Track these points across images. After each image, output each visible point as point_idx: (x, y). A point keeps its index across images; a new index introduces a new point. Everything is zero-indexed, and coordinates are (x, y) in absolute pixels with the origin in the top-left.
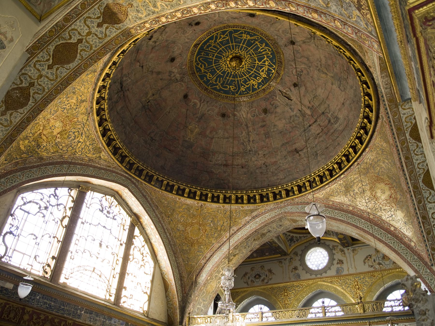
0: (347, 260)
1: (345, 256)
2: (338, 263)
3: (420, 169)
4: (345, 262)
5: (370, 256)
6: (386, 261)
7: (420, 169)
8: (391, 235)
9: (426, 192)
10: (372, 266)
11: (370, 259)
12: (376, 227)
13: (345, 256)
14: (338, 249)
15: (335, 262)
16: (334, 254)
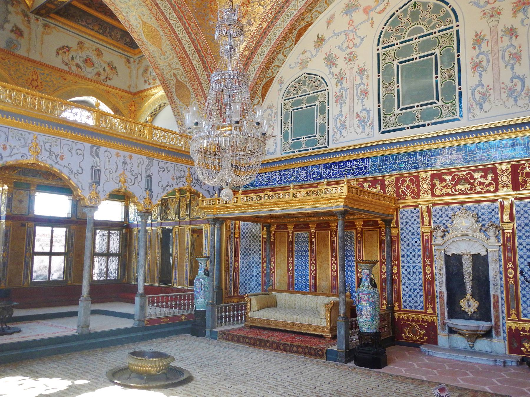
0: (30, 33)
1: (29, 27)
2: (12, 31)
3: (311, 17)
4: (25, 34)
5: (69, 49)
6: (87, 66)
7: (311, 17)
8: (199, 55)
9: (290, 42)
10: (67, 64)
11: (67, 53)
12: (187, 36)
13: (29, 27)
14: (20, 10)
15: (8, 27)
16: (10, 13)
